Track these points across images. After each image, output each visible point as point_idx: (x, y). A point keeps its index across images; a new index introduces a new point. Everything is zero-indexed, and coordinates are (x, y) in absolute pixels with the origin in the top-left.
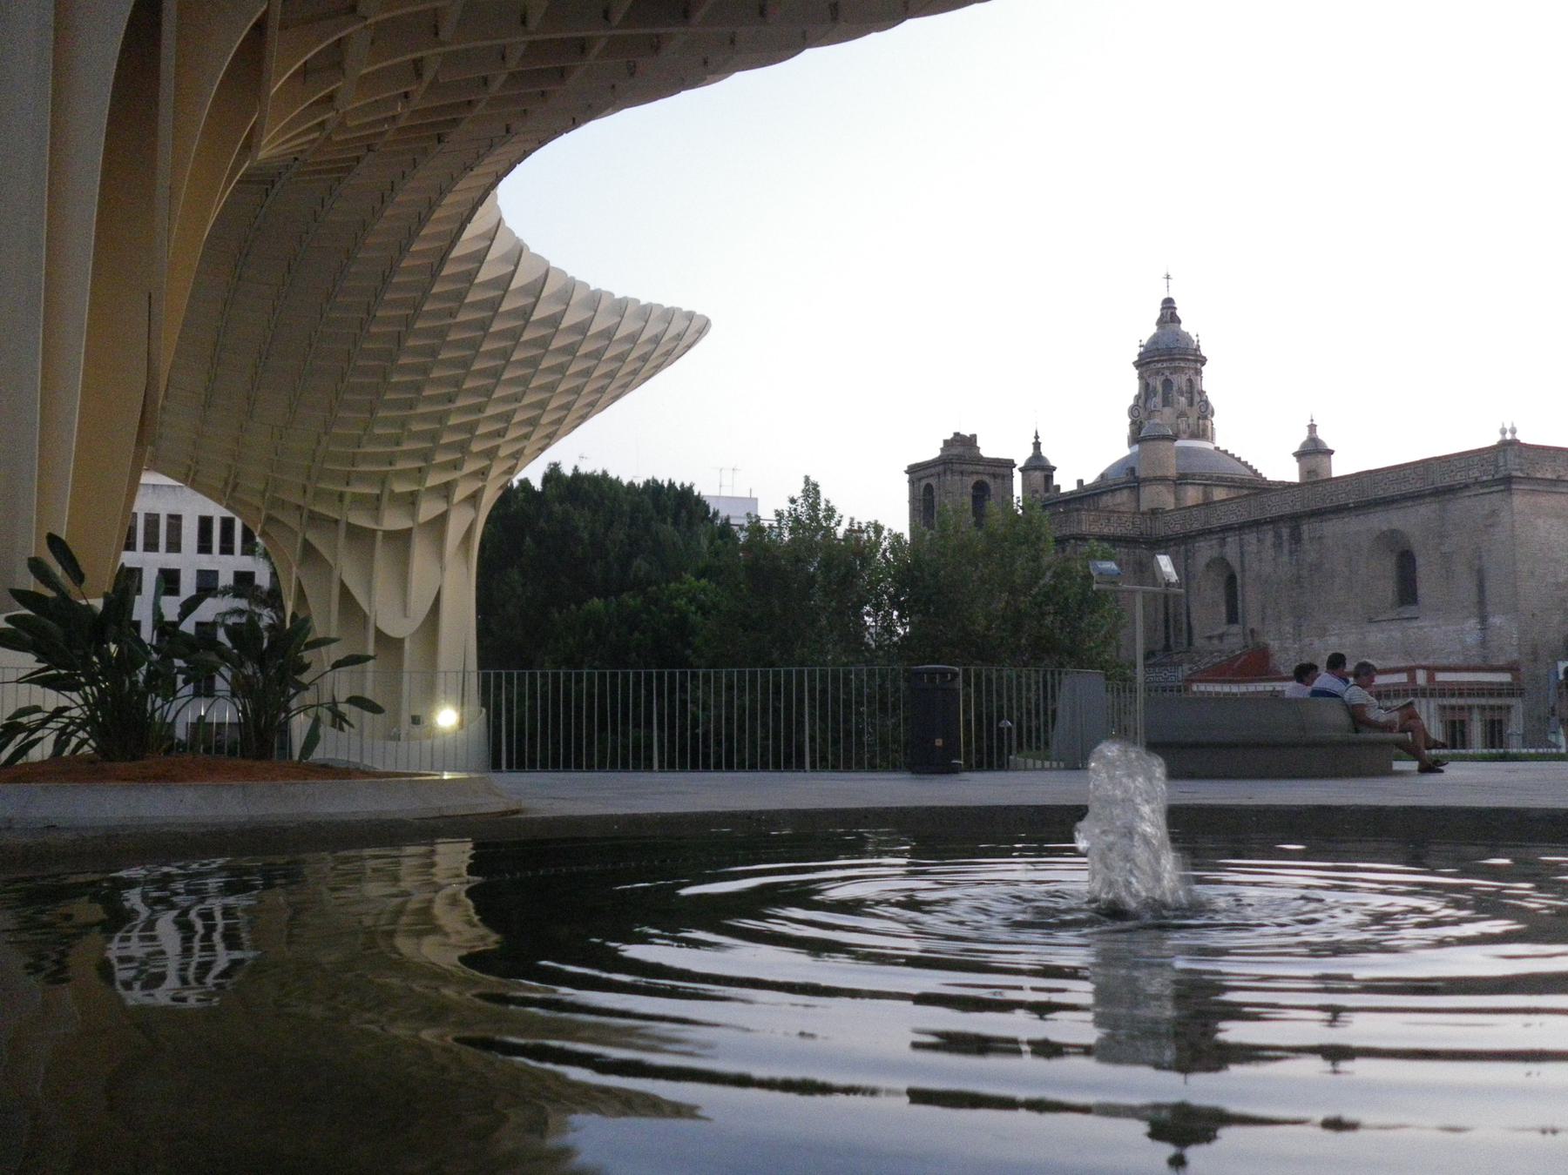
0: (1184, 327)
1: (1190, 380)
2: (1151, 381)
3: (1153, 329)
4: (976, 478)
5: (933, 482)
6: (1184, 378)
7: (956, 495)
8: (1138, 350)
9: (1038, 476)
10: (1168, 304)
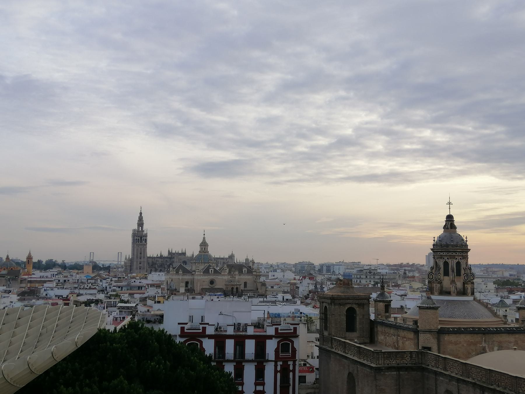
1: (458, 264)
2: (437, 261)
3: (441, 231)
4: (348, 306)
5: (328, 307)
6: (455, 261)
7: (339, 314)
8: (433, 242)
9: (381, 305)
10: (450, 218)
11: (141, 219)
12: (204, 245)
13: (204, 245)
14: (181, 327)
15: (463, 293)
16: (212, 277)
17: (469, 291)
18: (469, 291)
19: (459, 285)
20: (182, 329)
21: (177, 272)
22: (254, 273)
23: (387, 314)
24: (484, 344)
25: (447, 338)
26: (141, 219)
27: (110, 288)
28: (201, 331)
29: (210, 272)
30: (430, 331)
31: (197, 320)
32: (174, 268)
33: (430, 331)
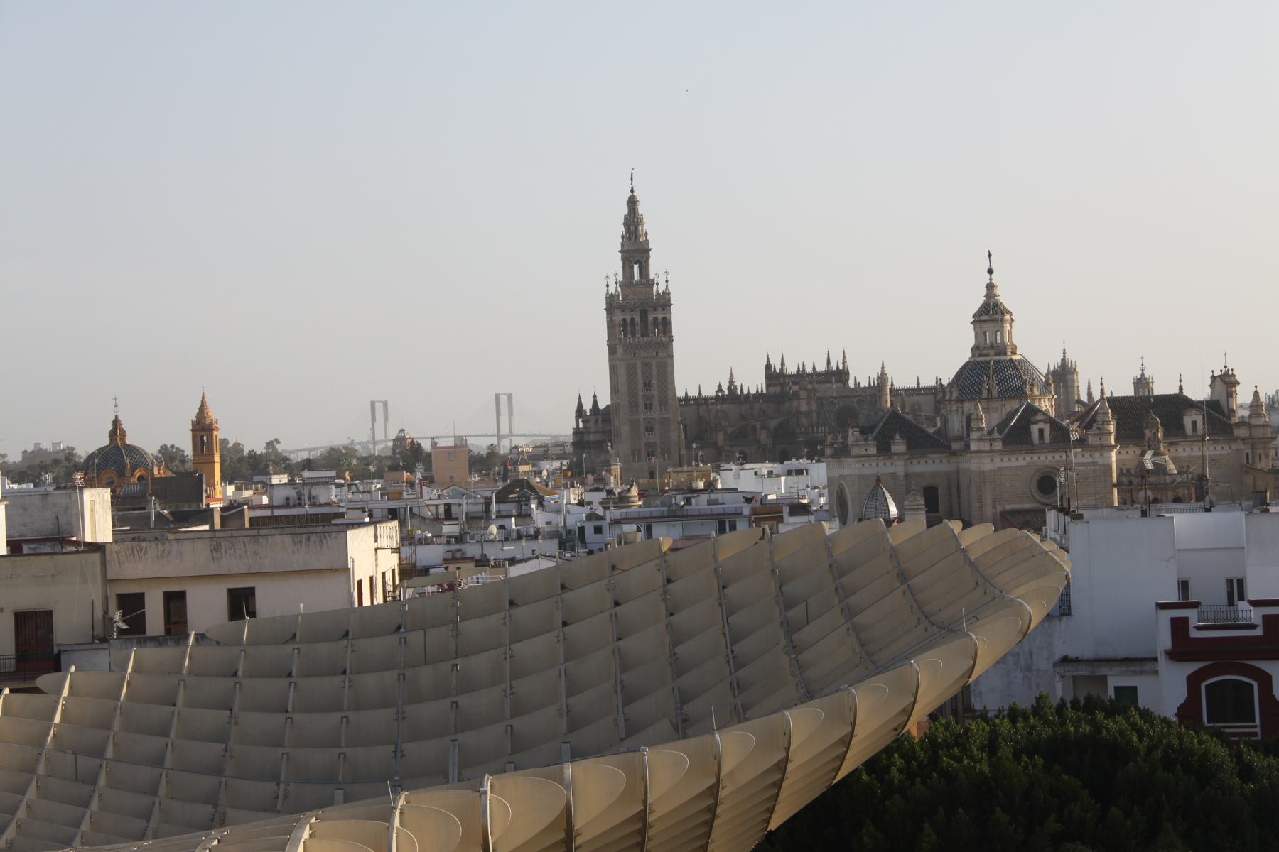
11: (633, 222)
12: (991, 314)
13: (991, 314)
14: (1173, 620)
16: (1044, 459)
20: (1179, 626)
21: (884, 449)
22: (1242, 432)
26: (633, 222)
27: (598, 530)
28: (1259, 632)
29: (1035, 435)
31: (1211, 593)
32: (864, 431)
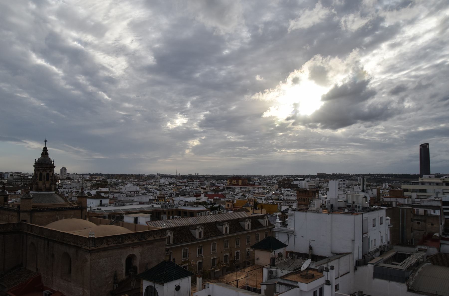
0: (50, 156)
1: (48, 174)
3: (40, 156)
6: (46, 173)
10: (45, 149)
15: (50, 190)
17: (53, 188)
18: (53, 188)
19: (47, 185)
23: (6, 203)
24: (57, 216)
25: (36, 214)
30: (26, 211)
33: (26, 211)
